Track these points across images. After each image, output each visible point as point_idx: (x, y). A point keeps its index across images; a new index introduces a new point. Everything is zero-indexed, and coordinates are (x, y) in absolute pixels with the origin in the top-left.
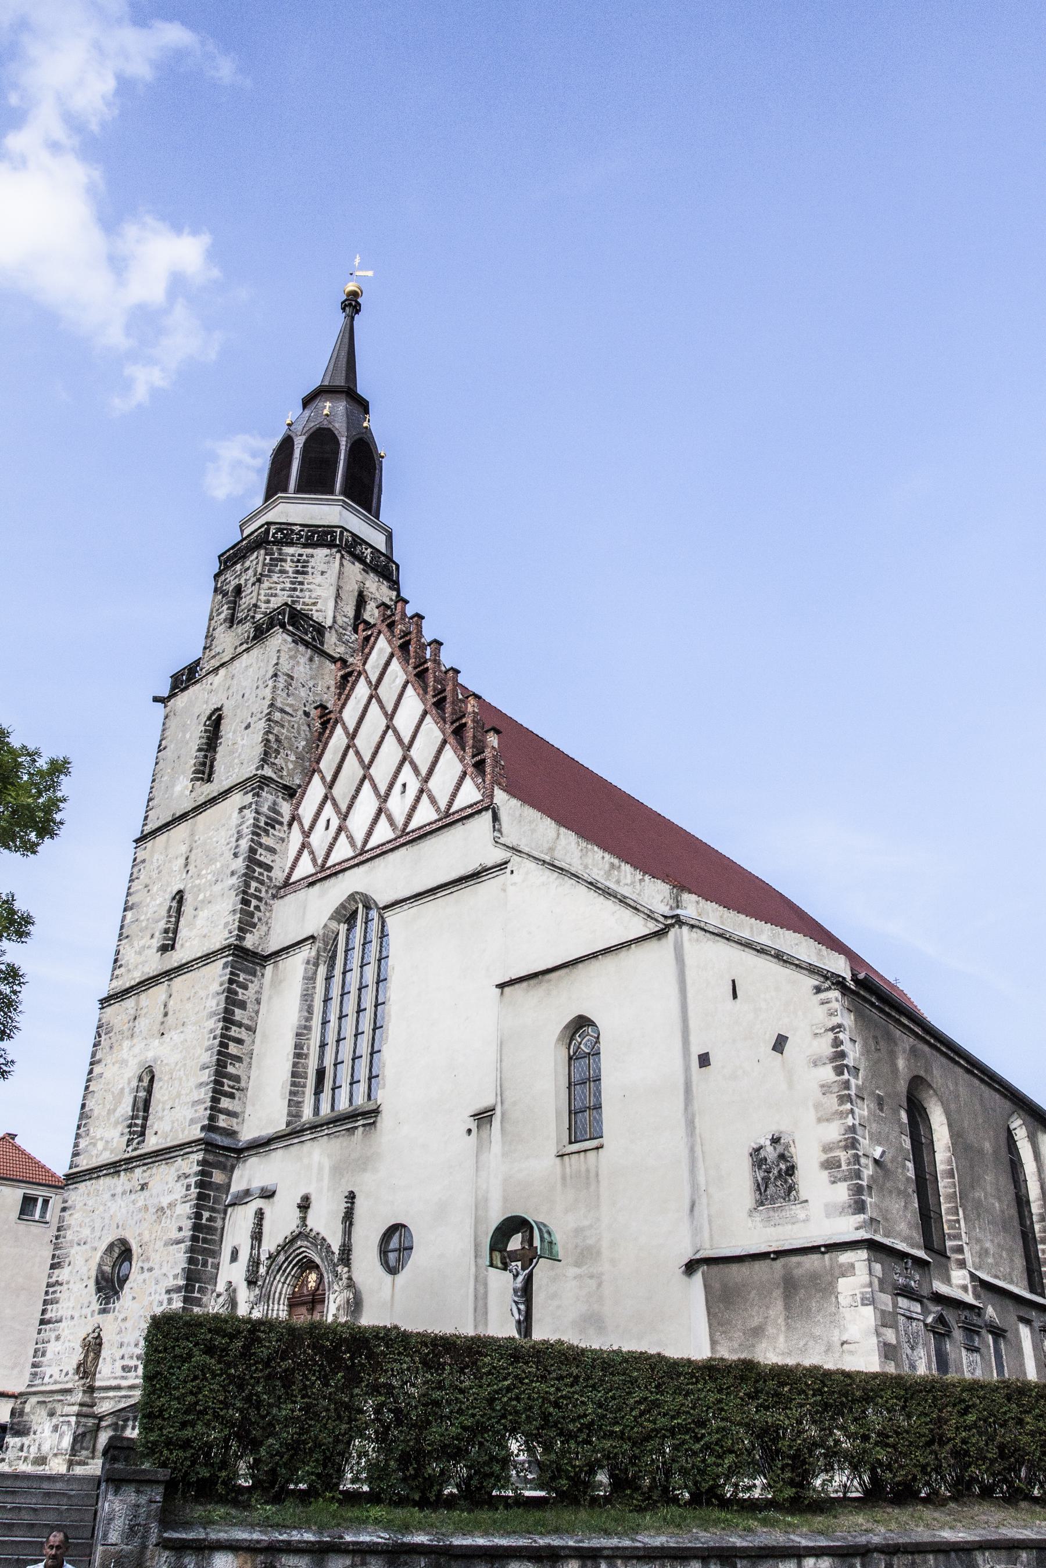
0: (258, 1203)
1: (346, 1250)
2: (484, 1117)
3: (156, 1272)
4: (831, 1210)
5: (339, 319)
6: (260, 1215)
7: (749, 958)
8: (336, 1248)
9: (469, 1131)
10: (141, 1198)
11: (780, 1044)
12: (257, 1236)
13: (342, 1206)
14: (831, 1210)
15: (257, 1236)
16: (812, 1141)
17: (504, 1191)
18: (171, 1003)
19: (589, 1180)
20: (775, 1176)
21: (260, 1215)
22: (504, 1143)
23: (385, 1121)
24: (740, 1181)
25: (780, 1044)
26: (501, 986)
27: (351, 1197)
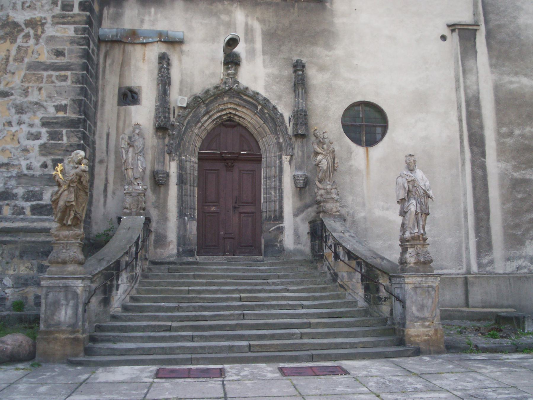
1: (301, 117)
9: (444, 38)
12: (164, 82)
13: (288, 72)
15: (164, 82)
17: (496, 96)
21: (163, 59)
22: (490, 57)
27: (299, 67)
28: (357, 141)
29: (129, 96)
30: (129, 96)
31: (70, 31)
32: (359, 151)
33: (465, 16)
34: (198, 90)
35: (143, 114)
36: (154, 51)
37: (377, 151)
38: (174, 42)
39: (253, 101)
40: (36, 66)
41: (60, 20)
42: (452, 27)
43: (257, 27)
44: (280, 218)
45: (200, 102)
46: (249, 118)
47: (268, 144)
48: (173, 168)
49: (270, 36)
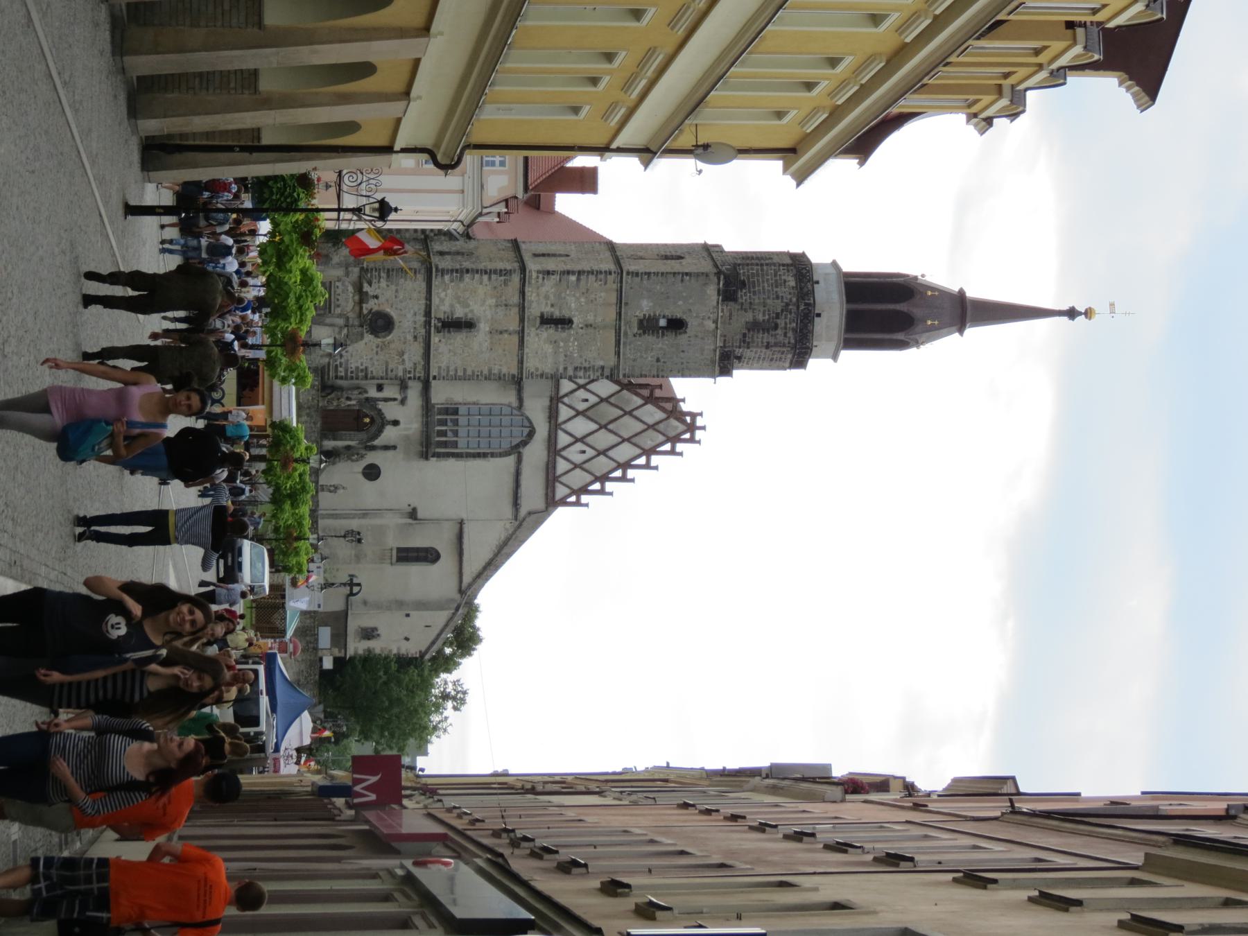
0: (399, 397)
1: (373, 448)
2: (413, 514)
3: (376, 357)
4: (356, 649)
5: (1065, 307)
6: (395, 399)
7: (437, 632)
8: (376, 442)
10: (410, 337)
11: (407, 639)
12: (386, 400)
14: (356, 649)
15: (386, 400)
16: (377, 646)
18: (506, 336)
19: (382, 559)
20: (369, 634)
21: (395, 399)
23: (423, 463)
24: (368, 623)
25: (407, 639)
26: (461, 523)
27: (394, 447)
28: (365, 468)
29: (380, 388)
30: (380, 388)
31: (400, 374)
32: (360, 469)
33: (420, 515)
34: (384, 411)
35: (373, 393)
36: (399, 397)
37: (361, 477)
38: (403, 402)
39: (380, 431)
40: (387, 363)
41: (405, 371)
42: (414, 510)
43: (410, 432)
44: (335, 439)
45: (380, 412)
46: (373, 429)
47: (363, 435)
48: (353, 402)
49: (407, 438)
